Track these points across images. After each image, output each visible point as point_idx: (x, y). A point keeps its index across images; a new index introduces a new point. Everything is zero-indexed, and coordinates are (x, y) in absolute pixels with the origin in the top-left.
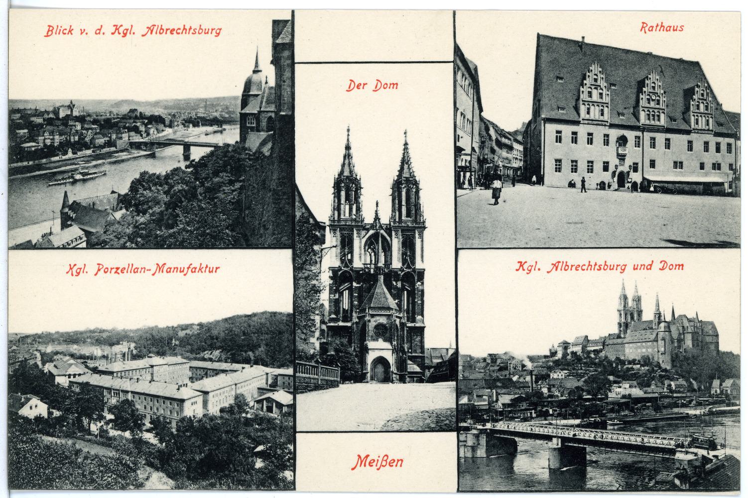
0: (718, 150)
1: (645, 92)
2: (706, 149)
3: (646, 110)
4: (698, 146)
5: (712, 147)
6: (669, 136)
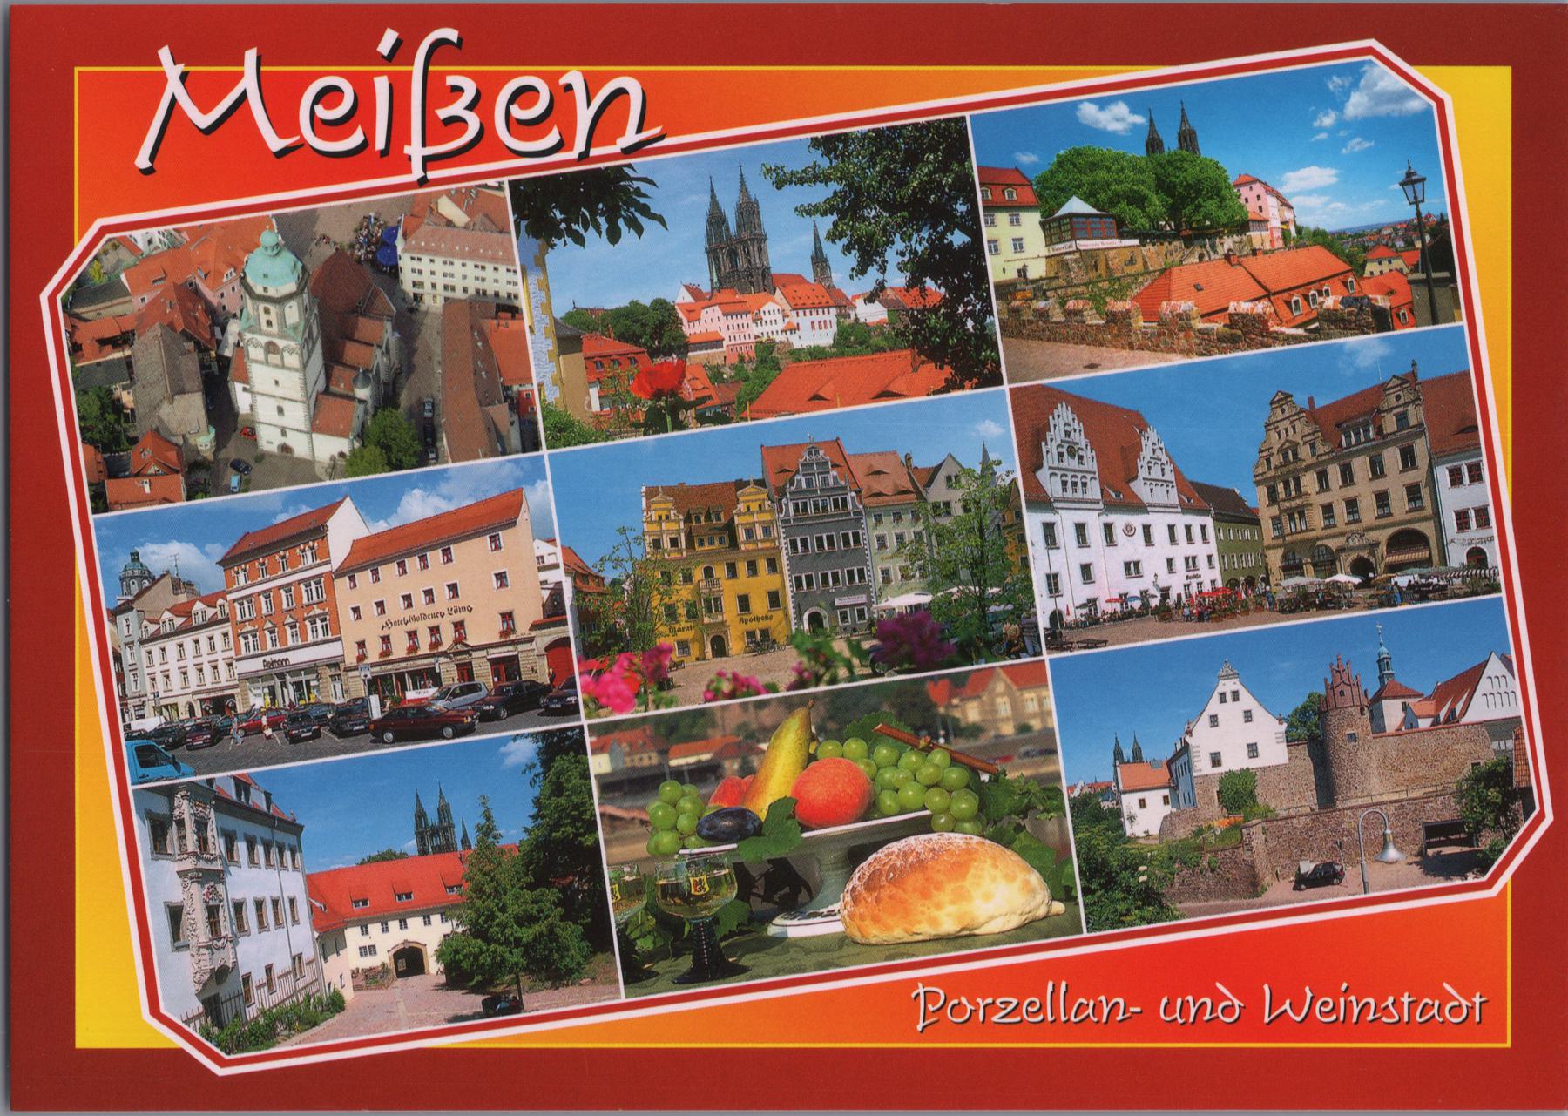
2: (1173, 540)
4: (1160, 534)
5: (1180, 534)
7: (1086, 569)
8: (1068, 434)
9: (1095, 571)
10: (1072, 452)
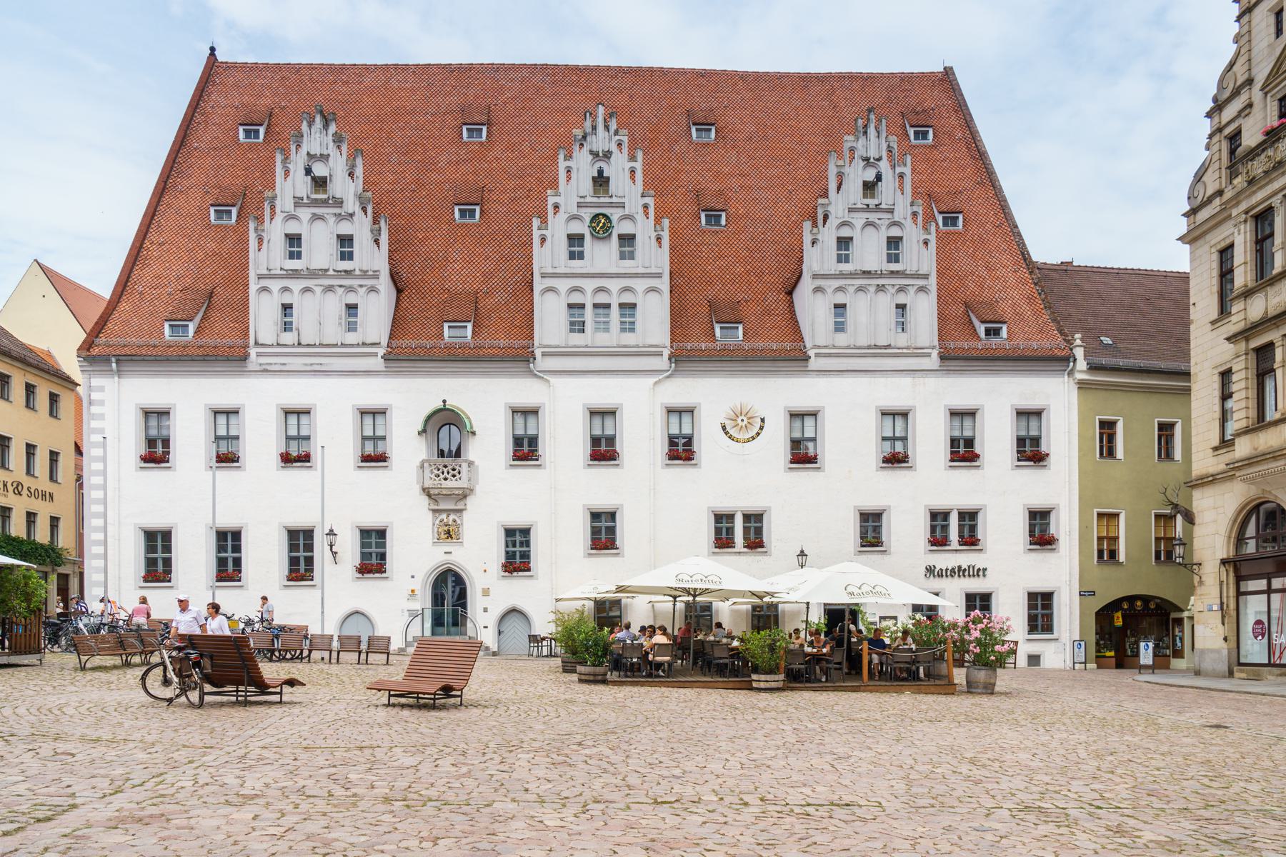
0: (964, 452)
1: (556, 207)
3: (563, 285)
5: (930, 439)
6: (685, 389)
7: (604, 532)
8: (601, 181)
9: (626, 531)
10: (601, 226)
